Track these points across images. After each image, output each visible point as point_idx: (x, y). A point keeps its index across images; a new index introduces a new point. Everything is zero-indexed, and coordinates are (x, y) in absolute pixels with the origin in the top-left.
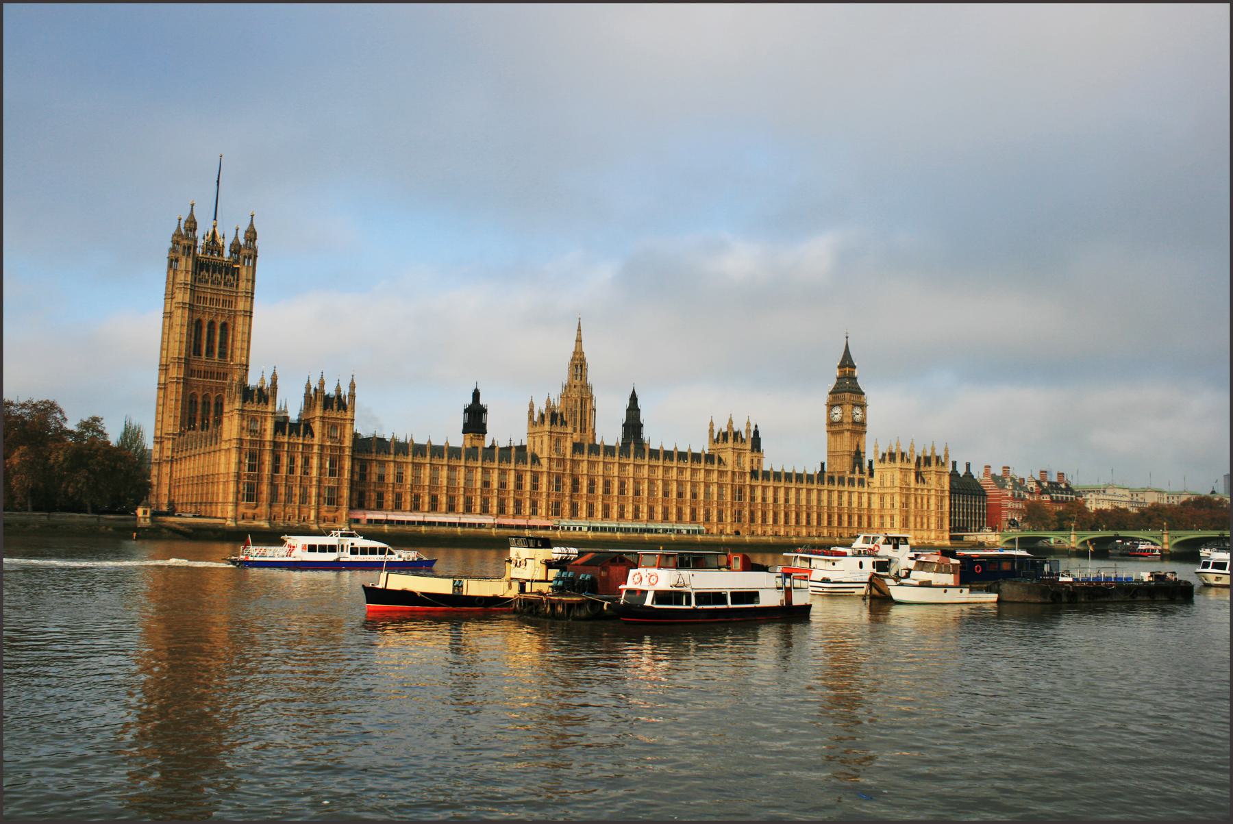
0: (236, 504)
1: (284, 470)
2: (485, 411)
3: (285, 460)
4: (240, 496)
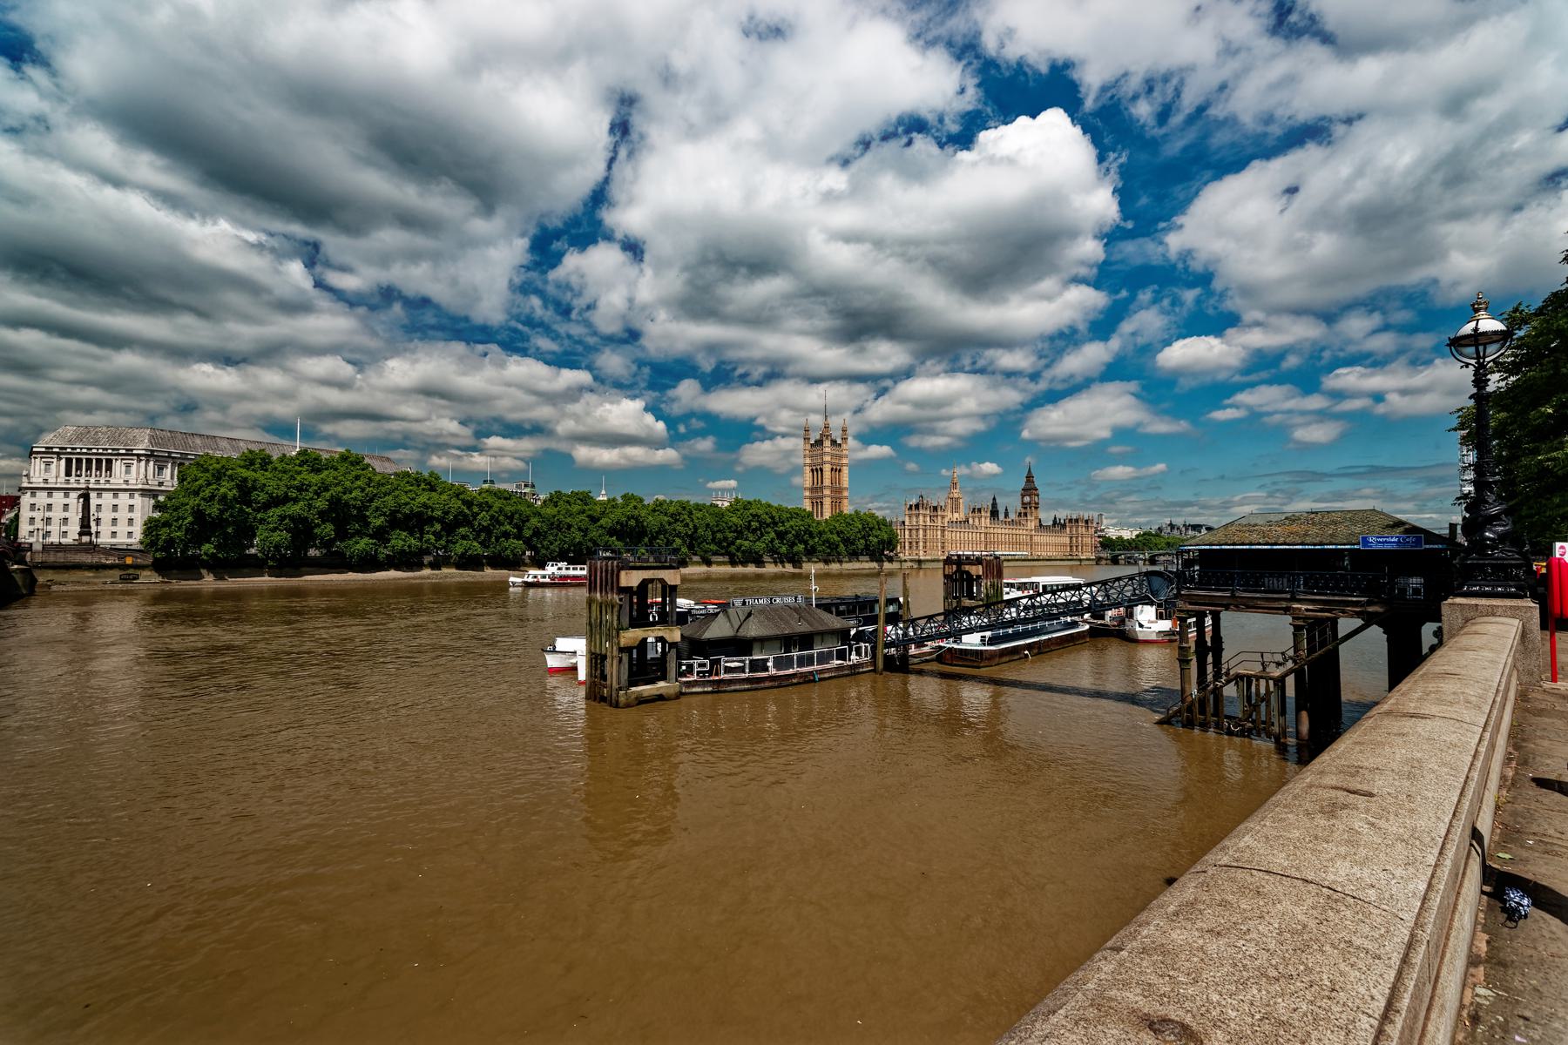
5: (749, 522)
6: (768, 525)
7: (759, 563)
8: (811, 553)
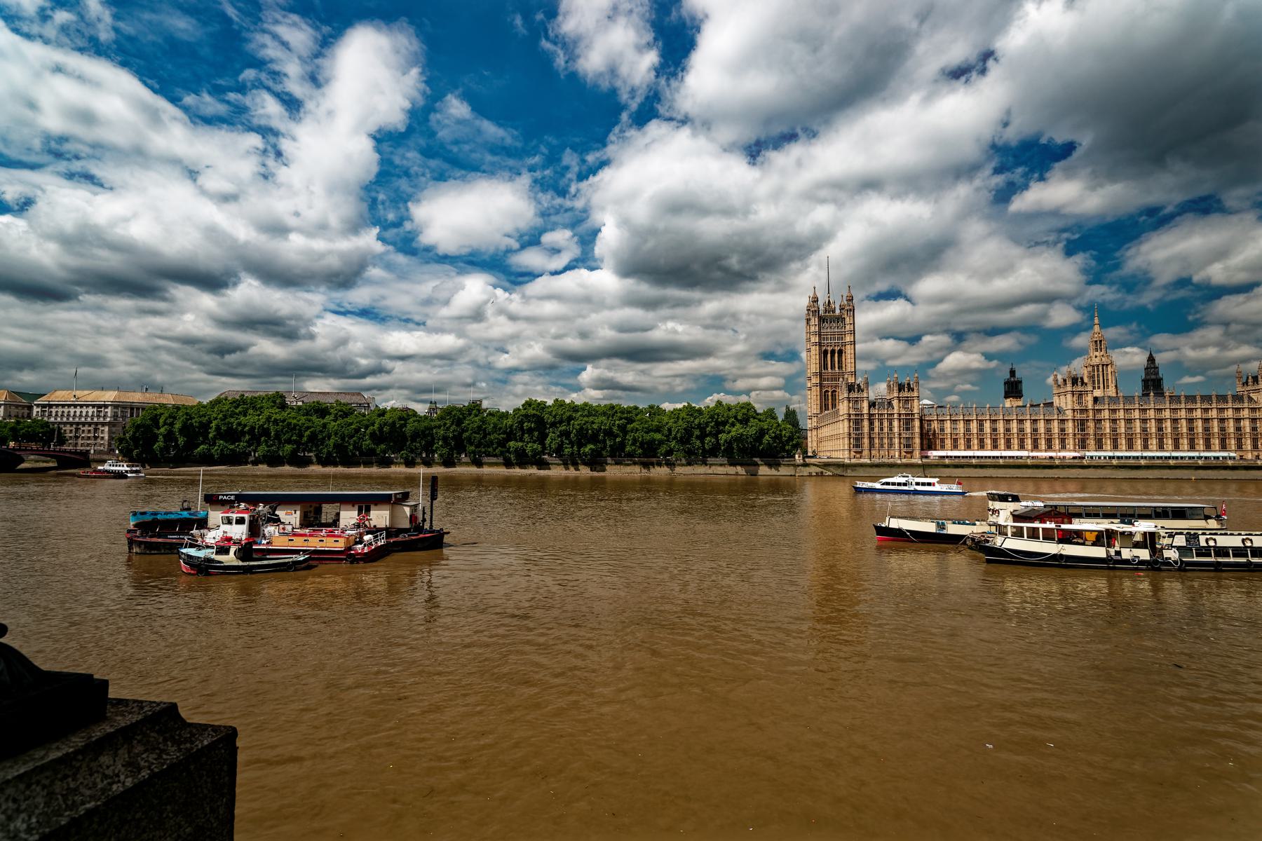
0: (850, 450)
1: (876, 430)
2: (1021, 382)
3: (877, 424)
4: (852, 446)
5: (521, 423)
6: (553, 425)
7: (543, 465)
8: (620, 455)
